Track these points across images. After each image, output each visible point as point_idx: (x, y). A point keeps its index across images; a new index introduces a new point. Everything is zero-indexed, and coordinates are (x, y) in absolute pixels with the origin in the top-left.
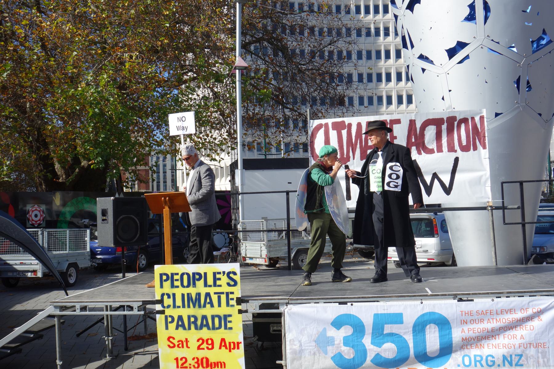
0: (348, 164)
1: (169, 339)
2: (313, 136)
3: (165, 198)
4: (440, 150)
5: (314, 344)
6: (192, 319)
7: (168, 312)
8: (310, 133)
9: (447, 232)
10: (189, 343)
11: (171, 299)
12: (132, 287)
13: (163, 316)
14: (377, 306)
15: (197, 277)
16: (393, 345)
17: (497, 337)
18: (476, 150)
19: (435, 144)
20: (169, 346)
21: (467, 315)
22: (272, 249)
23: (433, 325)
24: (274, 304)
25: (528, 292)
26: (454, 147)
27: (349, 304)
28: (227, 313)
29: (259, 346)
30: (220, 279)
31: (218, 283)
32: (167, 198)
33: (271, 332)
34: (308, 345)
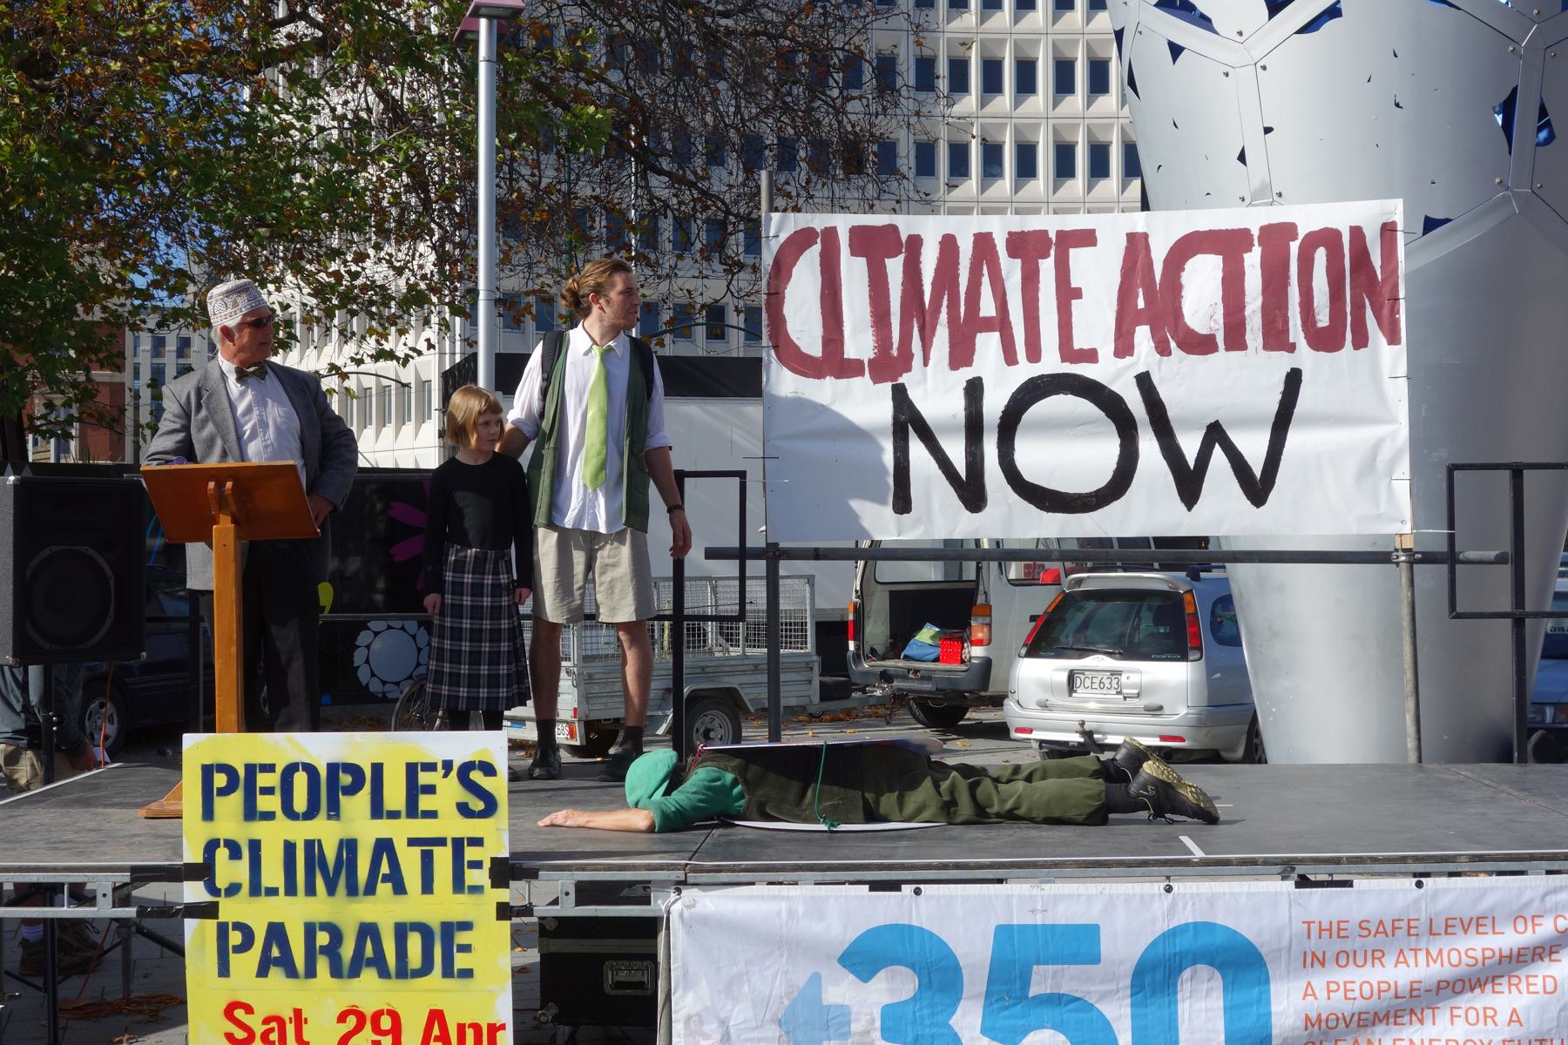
0: (904, 379)
1: (229, 1012)
2: (782, 270)
3: (220, 485)
4: (1235, 340)
5: (773, 1031)
6: (323, 939)
7: (230, 910)
8: (767, 259)
9: (1235, 641)
10: (305, 1027)
11: (244, 864)
12: (85, 818)
13: (211, 926)
14: (1009, 898)
15: (346, 779)
16: (1062, 1037)
17: (1428, 1013)
18: (1365, 345)
19: (1221, 321)
20: (229, 1036)
21: (1325, 934)
22: (596, 689)
23: (1203, 970)
24: (631, 884)
25: (1542, 858)
26: (1287, 331)
27: (907, 889)
28: (455, 916)
29: (561, 1040)
30: (430, 789)
31: (425, 803)
32: (229, 485)
33: (608, 990)
34: (755, 1034)
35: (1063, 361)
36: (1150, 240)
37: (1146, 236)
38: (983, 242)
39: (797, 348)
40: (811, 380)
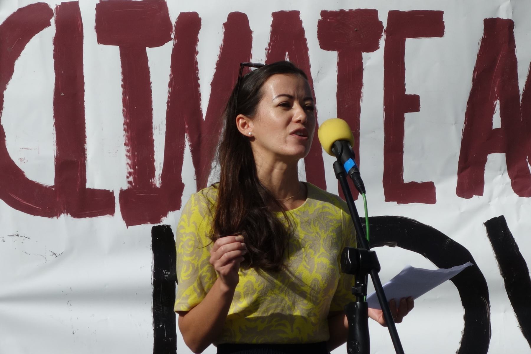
0: (170, 219)
35: (390, 196)
36: (517, 32)
37: (510, 24)
38: (286, 25)
39: (18, 173)
40: (39, 218)
